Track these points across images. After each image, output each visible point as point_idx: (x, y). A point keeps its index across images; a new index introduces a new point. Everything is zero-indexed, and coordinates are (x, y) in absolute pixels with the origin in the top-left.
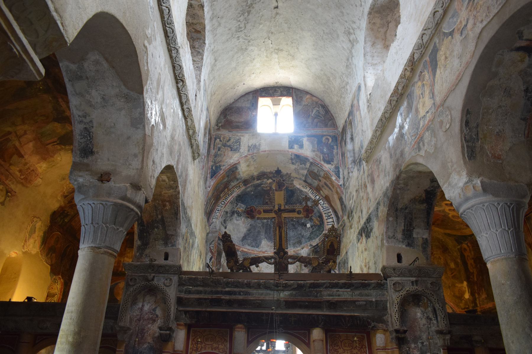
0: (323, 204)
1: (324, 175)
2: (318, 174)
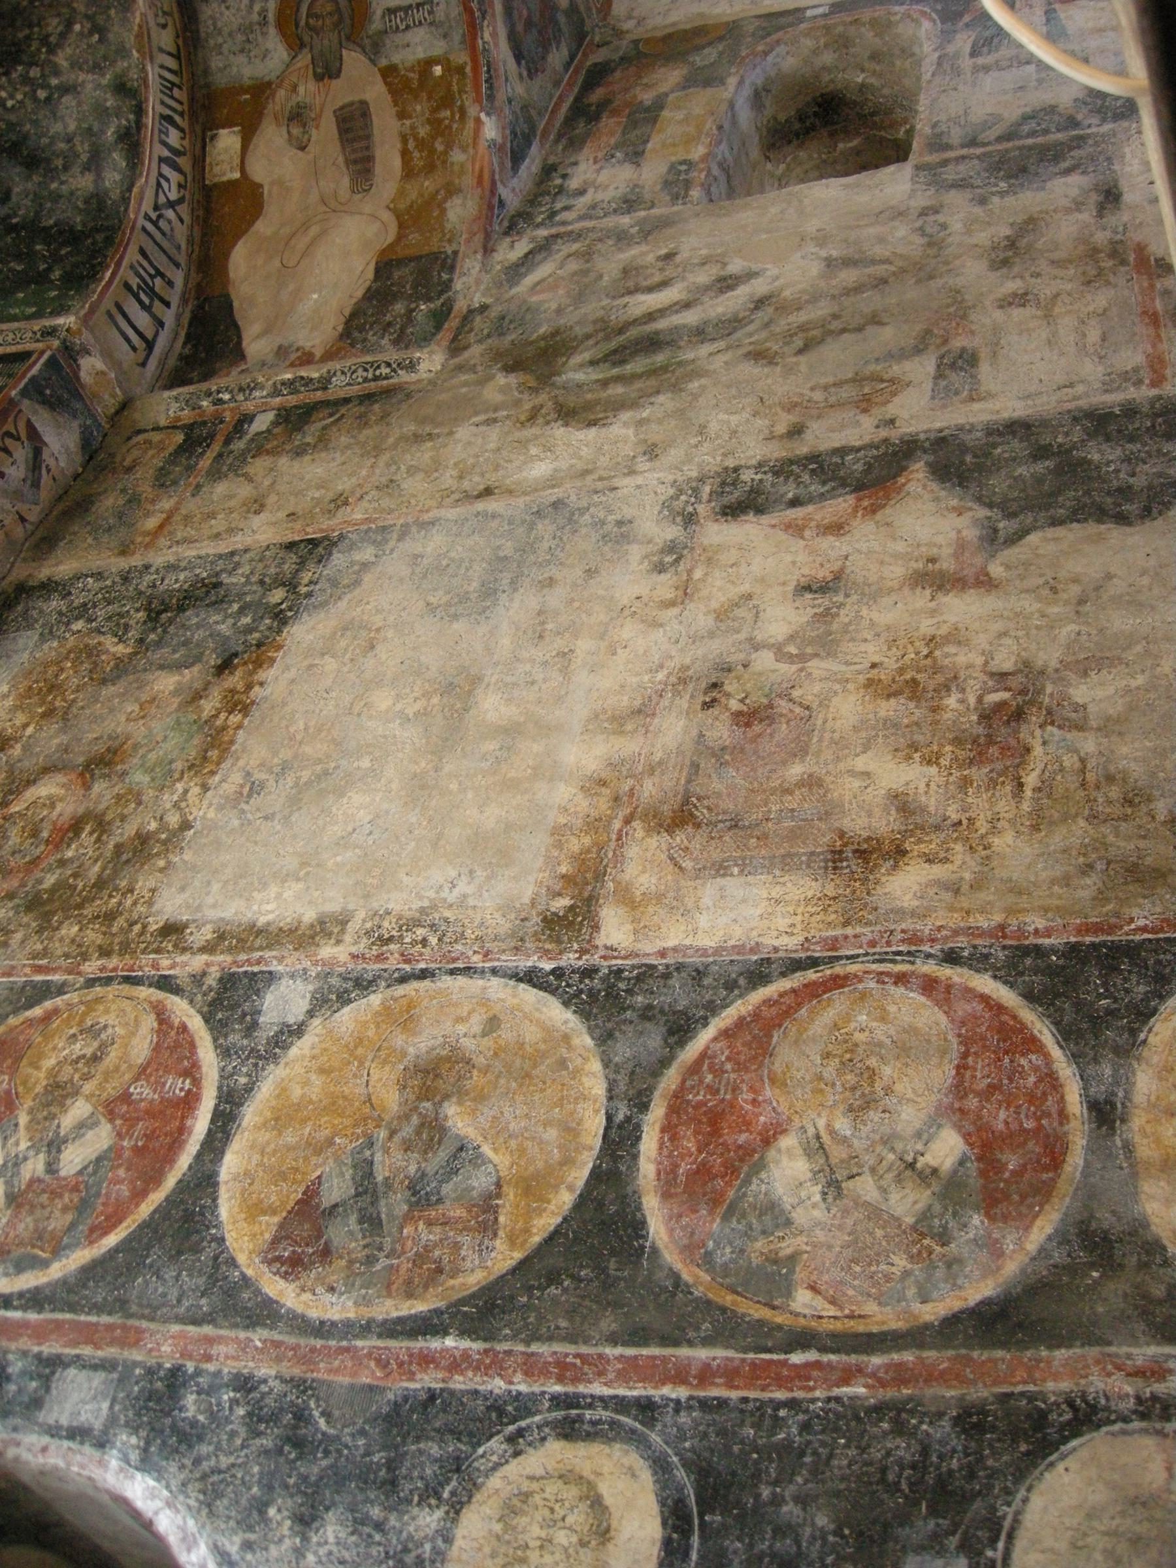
0: (171, 205)
1: (430, 62)
2: (376, 25)
